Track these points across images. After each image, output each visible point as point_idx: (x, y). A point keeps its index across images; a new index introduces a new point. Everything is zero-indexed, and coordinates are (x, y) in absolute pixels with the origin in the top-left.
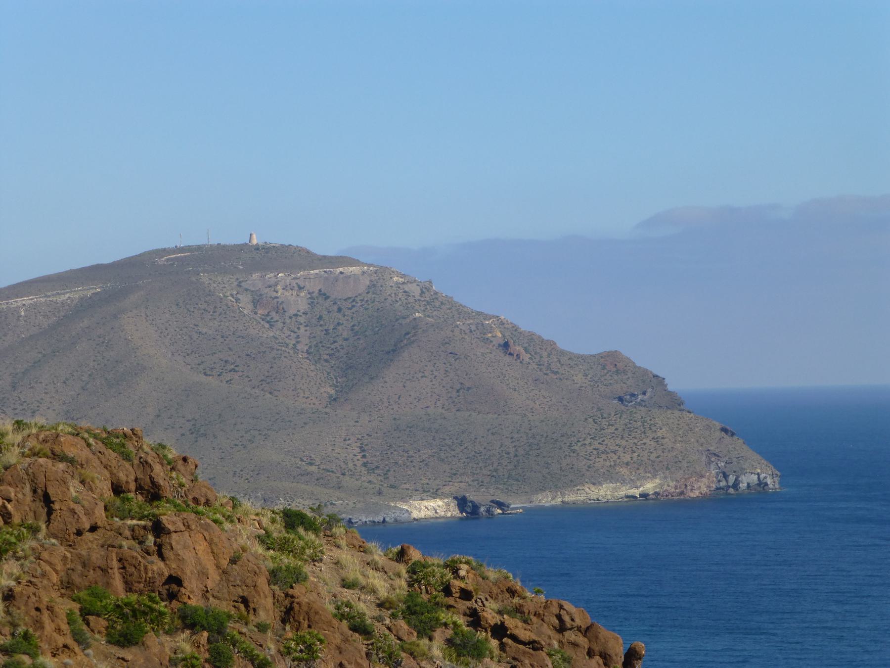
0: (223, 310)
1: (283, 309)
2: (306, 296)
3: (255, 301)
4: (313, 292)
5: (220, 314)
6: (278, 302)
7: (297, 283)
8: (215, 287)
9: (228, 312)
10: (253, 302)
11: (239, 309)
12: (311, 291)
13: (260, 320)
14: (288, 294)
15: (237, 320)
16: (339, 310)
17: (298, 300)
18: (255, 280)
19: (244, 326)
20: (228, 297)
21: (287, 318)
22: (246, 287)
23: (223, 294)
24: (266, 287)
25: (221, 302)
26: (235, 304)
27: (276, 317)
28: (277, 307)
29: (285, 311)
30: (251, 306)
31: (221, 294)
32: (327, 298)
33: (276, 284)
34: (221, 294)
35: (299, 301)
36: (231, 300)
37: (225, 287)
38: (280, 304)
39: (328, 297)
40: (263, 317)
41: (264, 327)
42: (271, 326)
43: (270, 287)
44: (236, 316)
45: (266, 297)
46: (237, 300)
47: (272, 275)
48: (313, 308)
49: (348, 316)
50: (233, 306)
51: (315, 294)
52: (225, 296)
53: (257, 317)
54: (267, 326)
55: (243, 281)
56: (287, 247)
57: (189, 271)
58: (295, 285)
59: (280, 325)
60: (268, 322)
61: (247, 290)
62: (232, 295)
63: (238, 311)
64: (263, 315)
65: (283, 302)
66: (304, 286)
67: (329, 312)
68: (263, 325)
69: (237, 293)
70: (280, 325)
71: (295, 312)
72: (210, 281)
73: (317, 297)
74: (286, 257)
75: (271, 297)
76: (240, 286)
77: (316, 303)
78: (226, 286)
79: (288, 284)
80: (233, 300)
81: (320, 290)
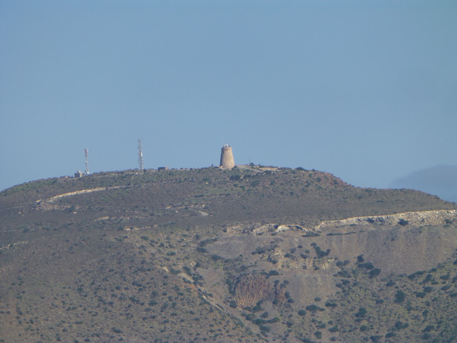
0: (170, 299)
1: (287, 295)
2: (332, 269)
3: (232, 280)
4: (346, 263)
5: (165, 307)
6: (277, 282)
7: (314, 245)
8: (153, 255)
9: (179, 304)
10: (228, 282)
11: (200, 296)
12: (342, 260)
13: (243, 319)
14: (296, 265)
15: (197, 319)
16: (400, 297)
17: (316, 279)
18: (232, 238)
19: (212, 331)
20: (179, 272)
21: (295, 314)
22: (215, 252)
23: (169, 266)
24: (253, 253)
25: (165, 284)
26: (192, 286)
27: (274, 313)
28: (276, 293)
29: (290, 301)
30: (223, 290)
31: (166, 269)
32: (374, 273)
33: (273, 247)
34: (166, 269)
35: (319, 280)
36: (184, 279)
37: (173, 254)
38: (282, 286)
39: (377, 272)
40: (247, 312)
41: (251, 334)
42: (264, 330)
43: (260, 251)
44: (195, 310)
45: (254, 272)
46: (197, 279)
47: (264, 228)
48: (346, 294)
49: (417, 309)
50: (188, 290)
51: (352, 266)
52: (172, 271)
53: (237, 313)
54: (256, 329)
55: (208, 241)
56: (294, 172)
57: (104, 222)
58: (310, 248)
59: (281, 328)
60: (258, 322)
61: (215, 258)
62: (187, 270)
63: (198, 301)
64: (248, 309)
65: (286, 282)
66: (329, 251)
67: (379, 302)
68: (247, 329)
69: (198, 265)
70: (281, 328)
71: (313, 302)
72: (144, 243)
73: (354, 272)
74: (292, 193)
75: (263, 273)
76: (203, 251)
77: (352, 283)
78: (176, 251)
79: (296, 245)
80: (189, 278)
81: (360, 258)
